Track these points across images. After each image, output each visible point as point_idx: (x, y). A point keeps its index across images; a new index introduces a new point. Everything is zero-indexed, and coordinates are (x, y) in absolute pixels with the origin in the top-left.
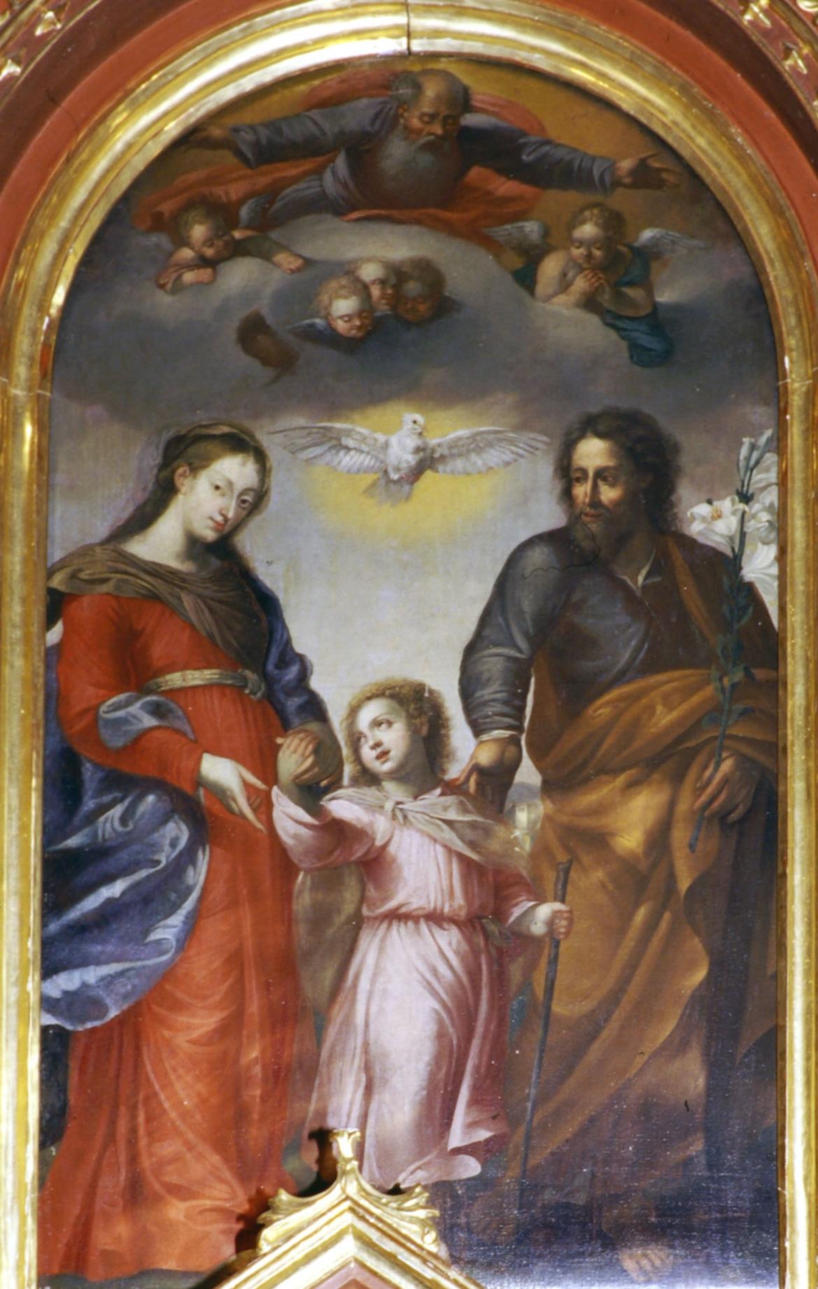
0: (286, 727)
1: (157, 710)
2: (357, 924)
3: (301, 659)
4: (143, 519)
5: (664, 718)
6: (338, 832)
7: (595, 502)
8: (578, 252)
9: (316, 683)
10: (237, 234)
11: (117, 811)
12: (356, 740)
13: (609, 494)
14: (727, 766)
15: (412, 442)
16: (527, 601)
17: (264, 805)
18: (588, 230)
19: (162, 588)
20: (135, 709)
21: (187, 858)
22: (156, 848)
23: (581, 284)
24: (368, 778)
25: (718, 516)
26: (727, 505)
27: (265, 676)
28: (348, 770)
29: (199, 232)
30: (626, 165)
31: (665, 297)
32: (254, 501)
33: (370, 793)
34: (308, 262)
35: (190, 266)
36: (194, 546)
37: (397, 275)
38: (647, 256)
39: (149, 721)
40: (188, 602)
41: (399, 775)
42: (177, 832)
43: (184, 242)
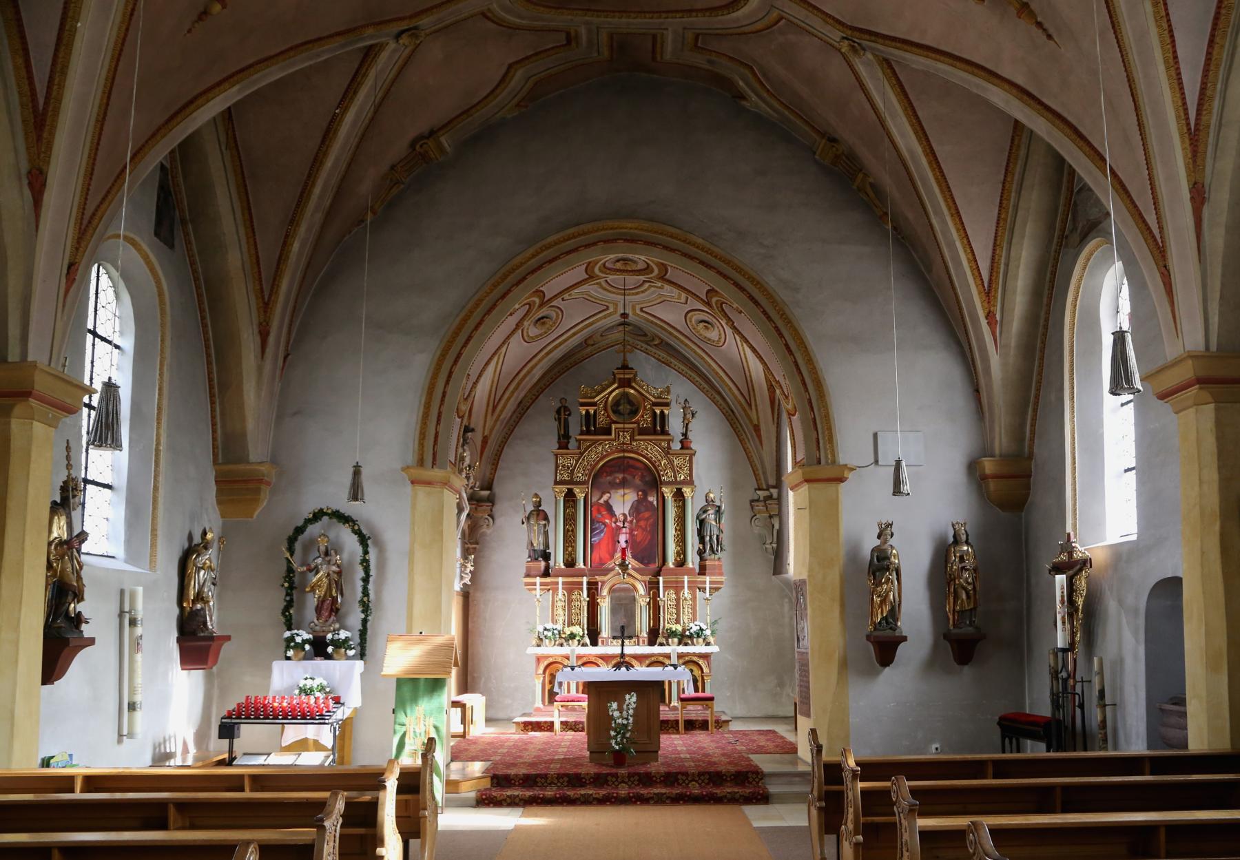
16: (635, 506)
32: (610, 498)
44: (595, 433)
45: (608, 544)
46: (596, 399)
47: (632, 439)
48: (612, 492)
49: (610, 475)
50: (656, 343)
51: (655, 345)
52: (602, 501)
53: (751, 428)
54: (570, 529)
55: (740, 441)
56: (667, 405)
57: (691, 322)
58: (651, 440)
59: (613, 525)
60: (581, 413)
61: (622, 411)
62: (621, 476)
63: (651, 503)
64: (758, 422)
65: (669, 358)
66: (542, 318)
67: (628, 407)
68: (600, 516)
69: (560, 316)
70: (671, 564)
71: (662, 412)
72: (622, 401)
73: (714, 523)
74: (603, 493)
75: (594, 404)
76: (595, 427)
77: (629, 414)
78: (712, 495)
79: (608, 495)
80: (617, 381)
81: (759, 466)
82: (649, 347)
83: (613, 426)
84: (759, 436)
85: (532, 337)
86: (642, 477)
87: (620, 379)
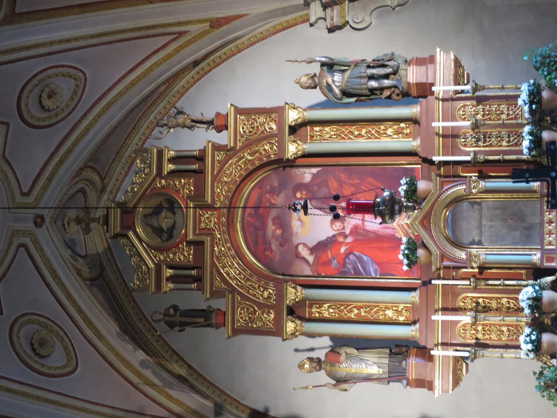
0: (336, 240)
1: (334, 259)
2: (364, 230)
3: (327, 238)
4: (307, 261)
5: (335, 184)
6: (351, 233)
7: (305, 195)
8: (271, 197)
9: (330, 235)
10: (268, 247)
11: (348, 266)
12: (338, 230)
13: (304, 193)
14: (342, 175)
15: (297, 222)
17: (347, 244)
18: (268, 196)
19: (317, 259)
20: (334, 263)
21: (355, 255)
22: (353, 260)
23: (275, 197)
24: (344, 228)
25: (307, 177)
26: (306, 175)
27: (329, 243)
28: (343, 231)
29: (267, 253)
30: (259, 191)
31: (277, 184)
32: (305, 245)
33: (346, 228)
34: (272, 237)
35: (272, 255)
36: (311, 254)
37: (274, 224)
38: (271, 187)
39: (336, 261)
40: (319, 255)
41: (343, 223)
42: (351, 257)
43: (269, 255)
44: (200, 268)
45: (380, 249)
46: (151, 265)
47: (210, 207)
48: (296, 241)
49: (270, 244)
50: (96, 178)
51: (102, 179)
52: (311, 259)
53: (217, 32)
54: (356, 311)
55: (239, 51)
56: (160, 153)
57: (44, 120)
58: (214, 178)
59: (349, 240)
60: (171, 290)
61: (170, 225)
62: (271, 227)
63: (314, 176)
64: (205, 21)
65: (123, 160)
66: (32, 344)
67: (163, 214)
68: (335, 262)
69: (33, 317)
70: (413, 144)
71: (172, 160)
72: (155, 223)
73: (347, 74)
74: (298, 256)
75: (158, 267)
76: (193, 268)
77: (174, 213)
78: (304, 80)
79: (300, 248)
80: (124, 232)
81: (276, 22)
82: (108, 189)
83: (191, 237)
84: (228, 20)
85: (69, 360)
86: (274, 192)
87: (122, 227)
